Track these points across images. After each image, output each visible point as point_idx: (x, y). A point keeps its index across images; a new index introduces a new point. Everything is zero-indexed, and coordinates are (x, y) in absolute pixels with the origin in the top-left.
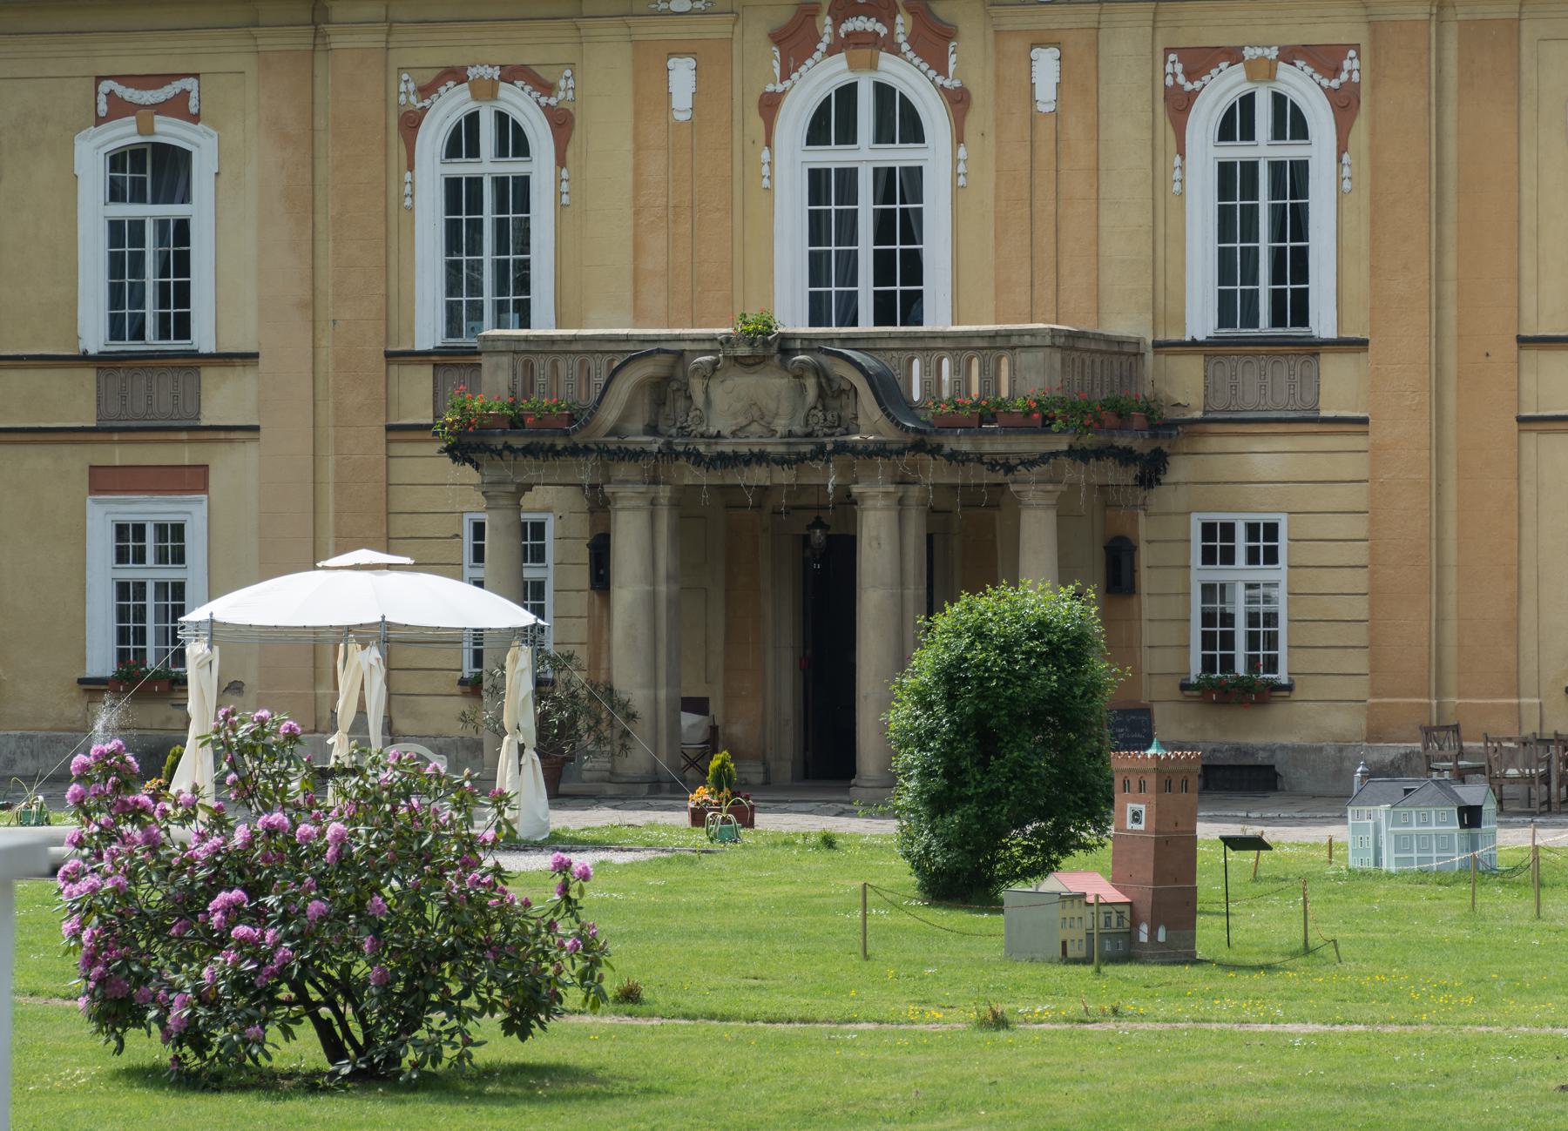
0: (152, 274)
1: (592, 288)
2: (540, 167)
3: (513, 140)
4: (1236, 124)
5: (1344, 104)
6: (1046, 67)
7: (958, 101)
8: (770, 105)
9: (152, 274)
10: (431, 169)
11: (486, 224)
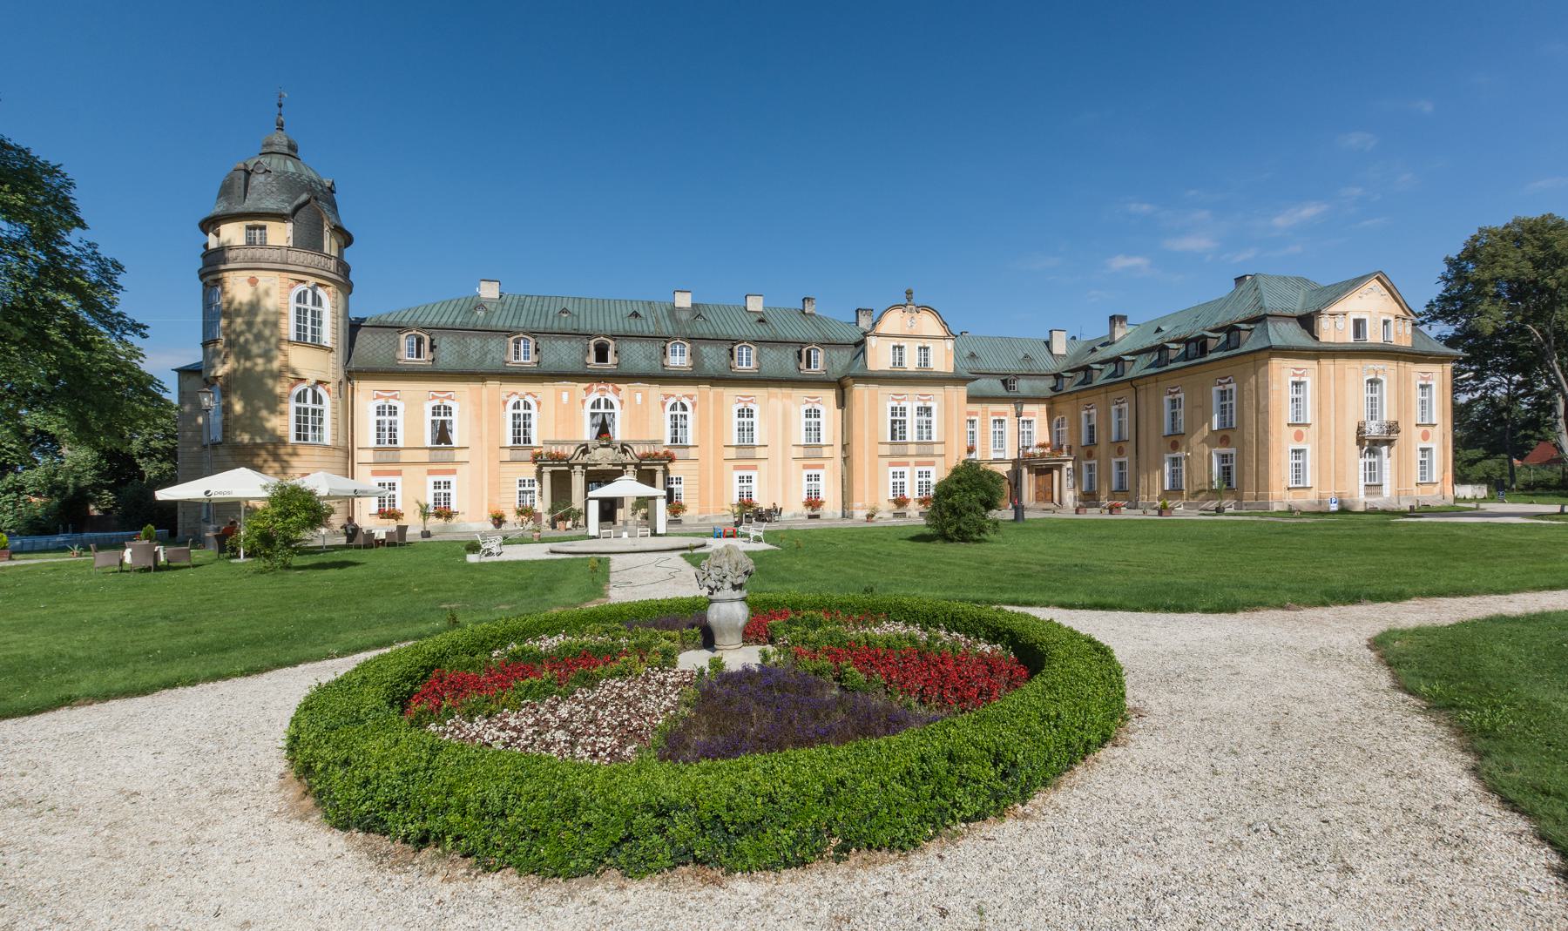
2: (534, 411)
3: (527, 406)
4: (673, 407)
5: (694, 405)
6: (639, 397)
7: (622, 402)
8: (583, 402)
10: (510, 411)
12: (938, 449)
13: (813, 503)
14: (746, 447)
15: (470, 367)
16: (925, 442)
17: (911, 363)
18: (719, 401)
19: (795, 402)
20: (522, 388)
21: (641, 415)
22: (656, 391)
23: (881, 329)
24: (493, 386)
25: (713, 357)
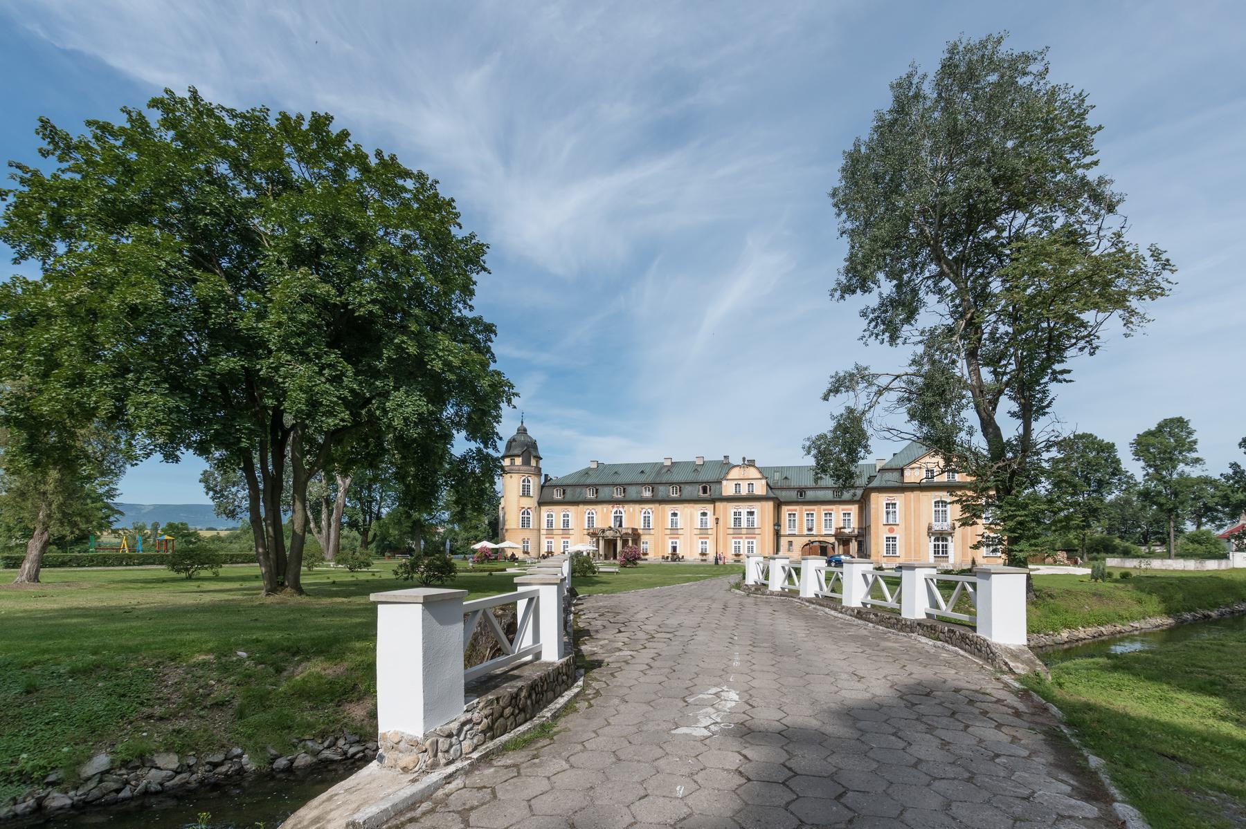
0: (566, 523)
1: (599, 524)
9: (566, 523)
11: (591, 520)
12: (757, 531)
13: (703, 554)
14: (674, 530)
15: (575, 499)
16: (751, 527)
17: (744, 491)
18: (663, 510)
19: (696, 510)
20: (590, 507)
21: (633, 516)
22: (637, 507)
23: (729, 477)
24: (581, 507)
25: (662, 491)
